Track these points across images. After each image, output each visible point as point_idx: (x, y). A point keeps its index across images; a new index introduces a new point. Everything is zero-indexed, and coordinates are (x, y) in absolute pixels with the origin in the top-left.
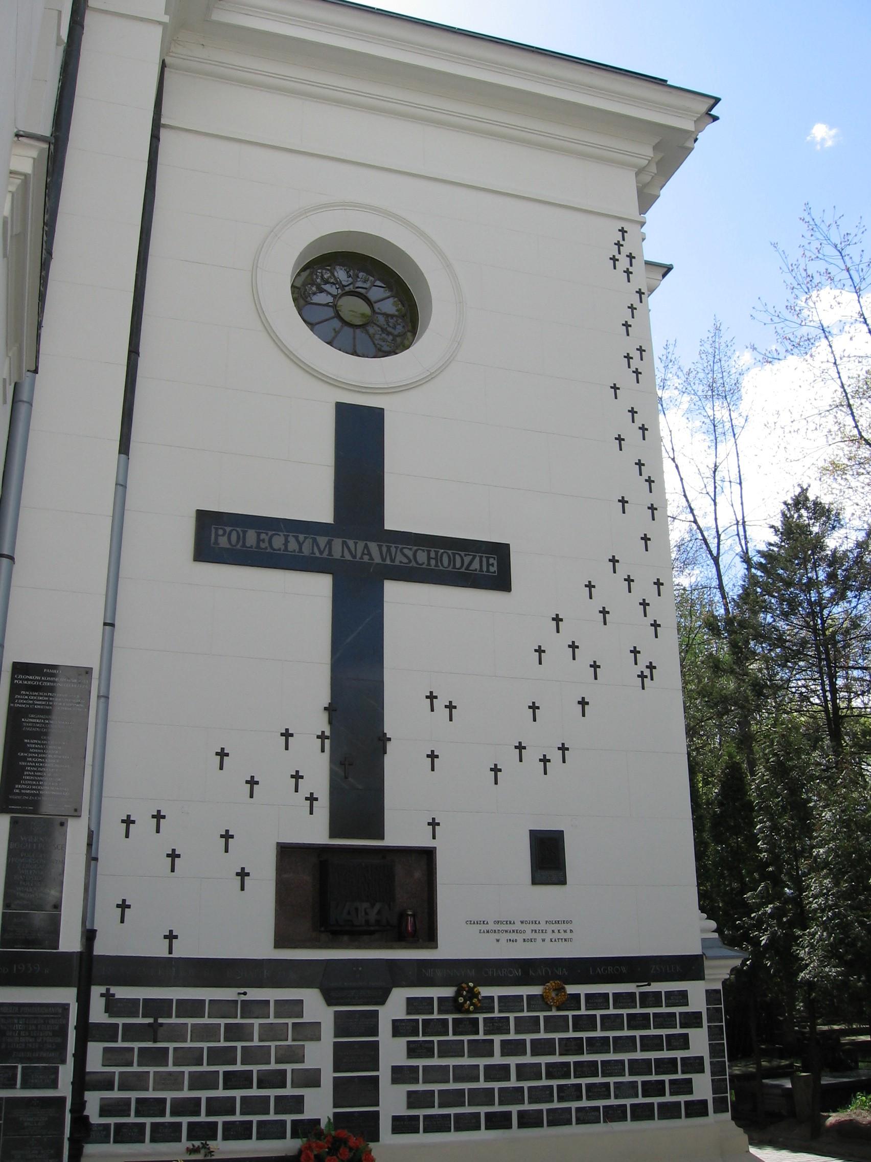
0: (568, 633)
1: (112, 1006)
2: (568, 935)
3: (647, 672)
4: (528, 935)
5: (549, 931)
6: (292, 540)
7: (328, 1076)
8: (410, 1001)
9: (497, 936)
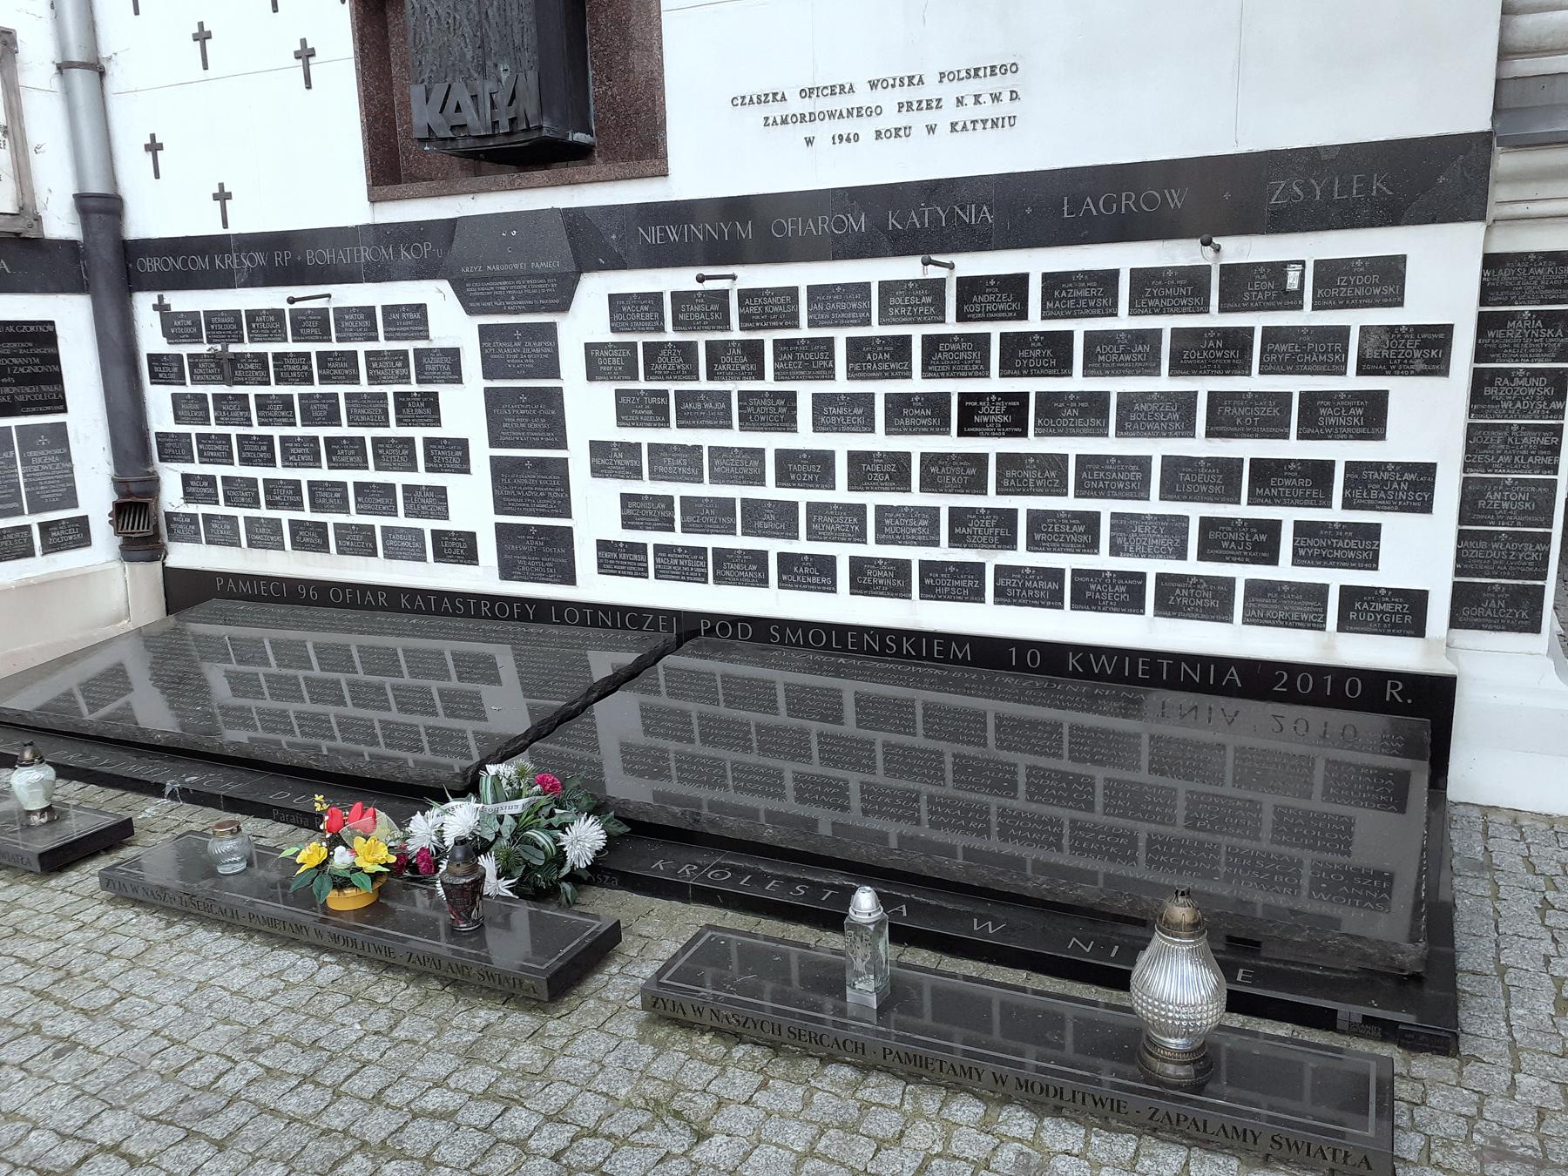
1: (174, 326)
2: (1005, 108)
5: (949, 102)
7: (481, 454)
9: (806, 130)
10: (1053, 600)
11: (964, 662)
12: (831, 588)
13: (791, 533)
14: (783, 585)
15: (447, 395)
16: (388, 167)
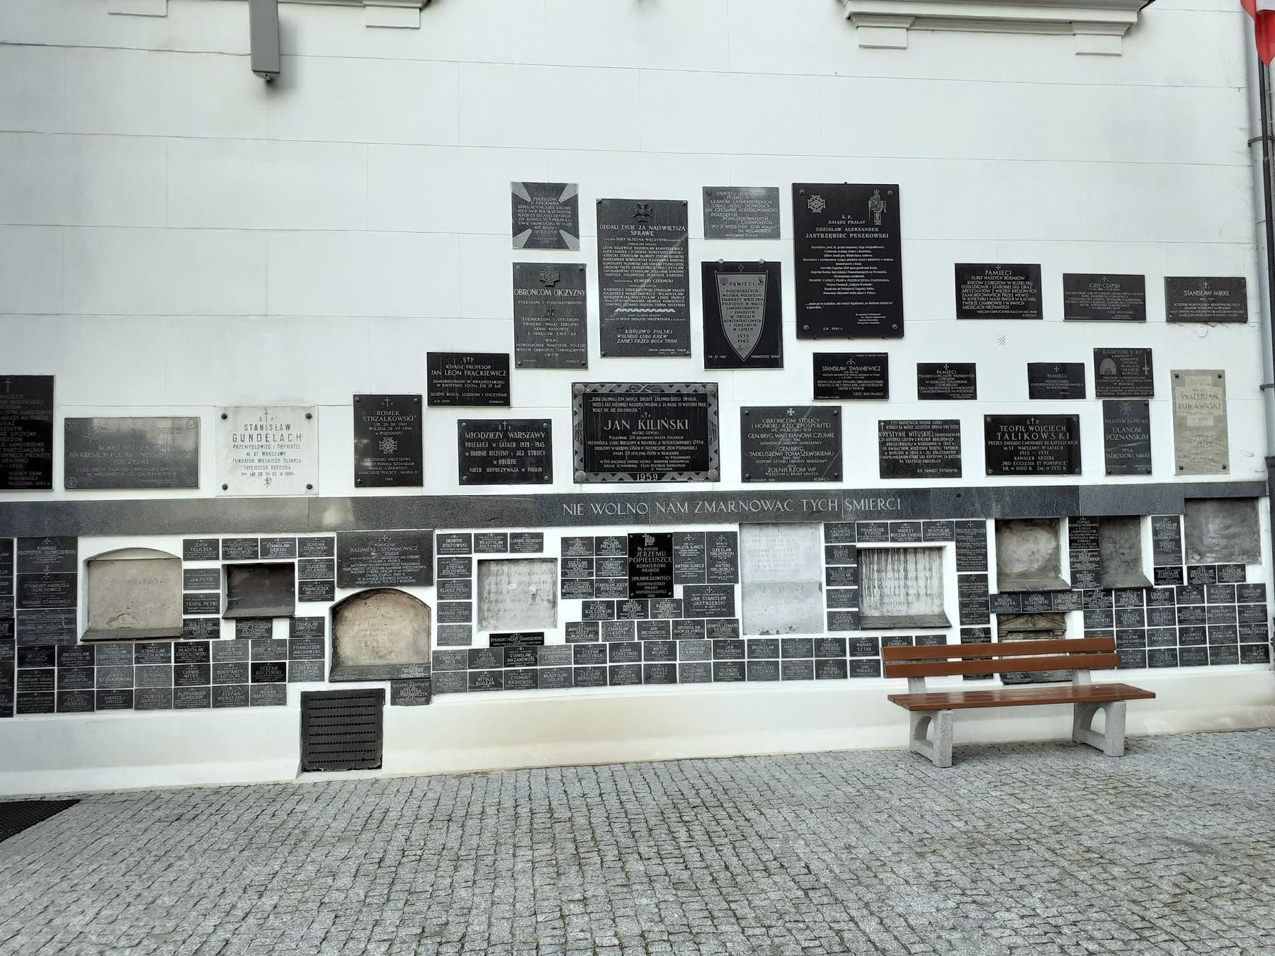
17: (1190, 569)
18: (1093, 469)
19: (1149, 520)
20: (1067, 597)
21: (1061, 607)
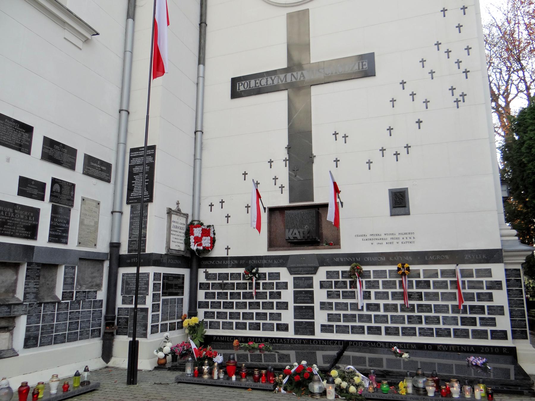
0: (409, 88)
1: (208, 276)
2: (412, 240)
3: (461, 98)
4: (389, 240)
5: (401, 238)
6: (269, 80)
7: (291, 305)
8: (328, 272)
9: (371, 241)
10: (432, 335)
11: (414, 349)
12: (380, 334)
13: (370, 321)
14: (368, 333)
15: (283, 292)
16: (271, 245)
17: (77, 292)
18: (42, 239)
19: (63, 267)
20: (20, 307)
21: (16, 313)
